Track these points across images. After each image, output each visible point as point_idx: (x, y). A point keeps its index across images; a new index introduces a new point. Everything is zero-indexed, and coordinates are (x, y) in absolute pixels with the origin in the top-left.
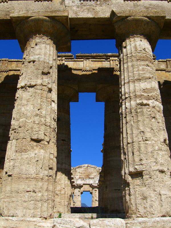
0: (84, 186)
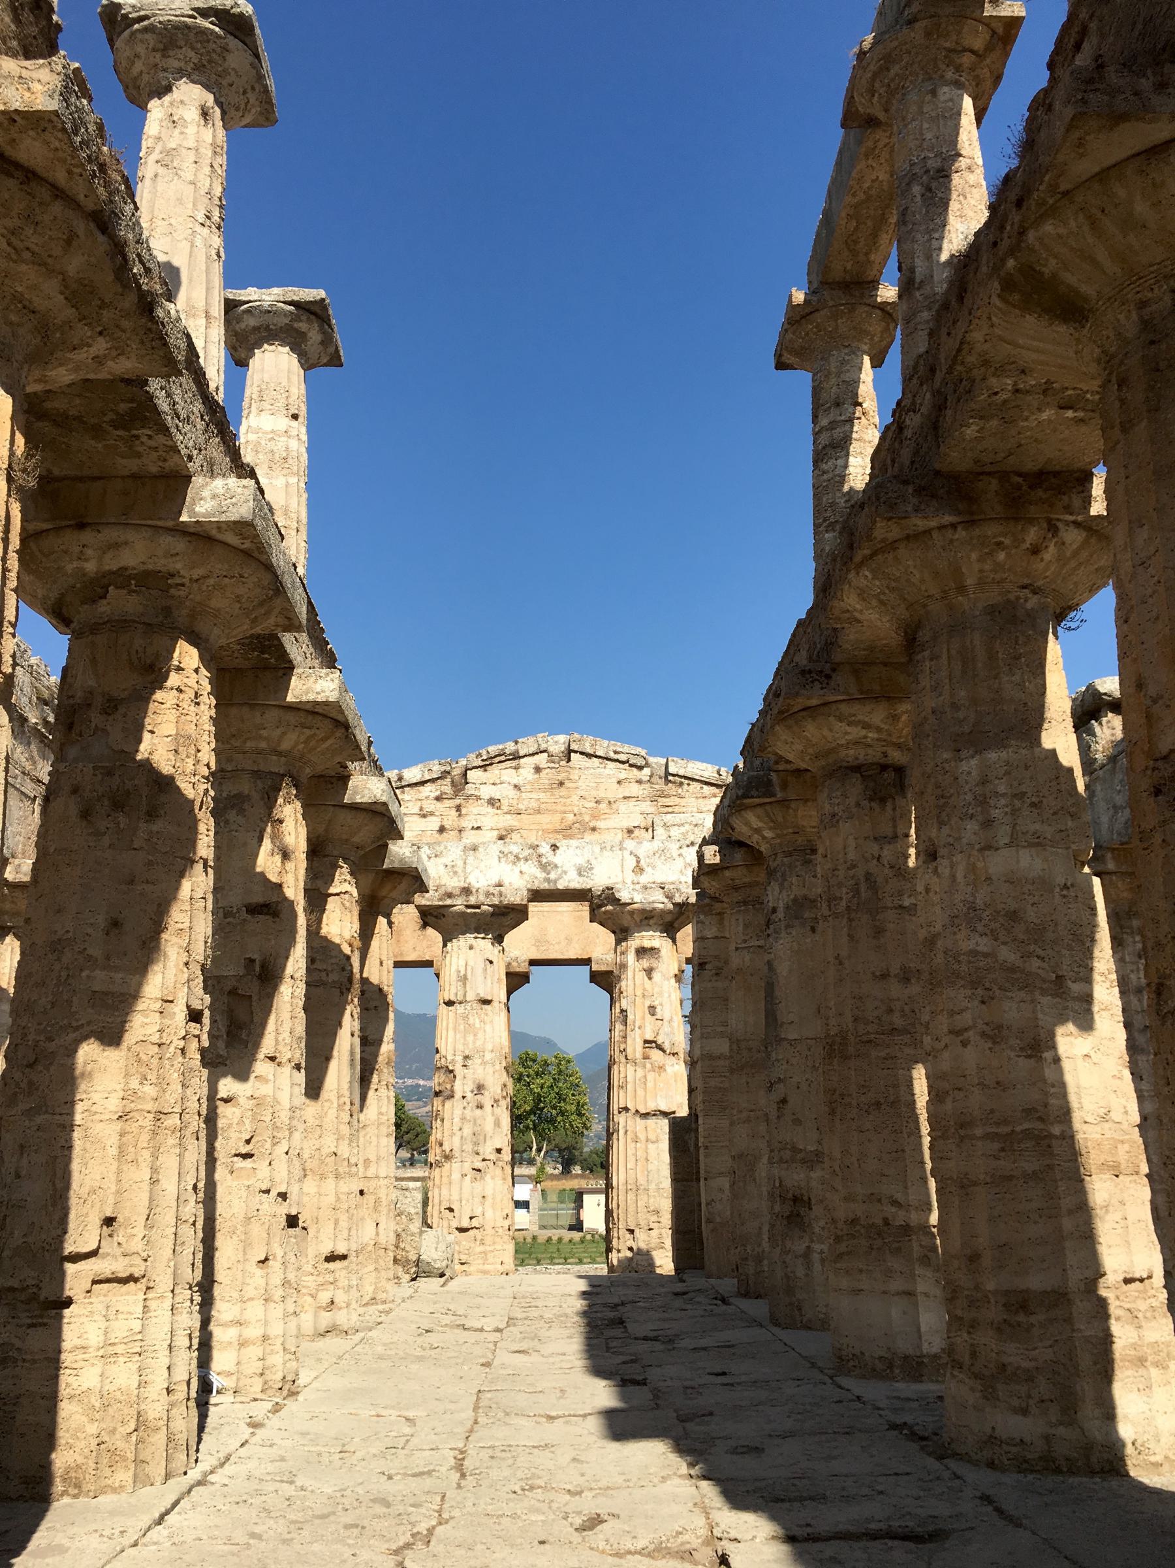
0: (533, 908)
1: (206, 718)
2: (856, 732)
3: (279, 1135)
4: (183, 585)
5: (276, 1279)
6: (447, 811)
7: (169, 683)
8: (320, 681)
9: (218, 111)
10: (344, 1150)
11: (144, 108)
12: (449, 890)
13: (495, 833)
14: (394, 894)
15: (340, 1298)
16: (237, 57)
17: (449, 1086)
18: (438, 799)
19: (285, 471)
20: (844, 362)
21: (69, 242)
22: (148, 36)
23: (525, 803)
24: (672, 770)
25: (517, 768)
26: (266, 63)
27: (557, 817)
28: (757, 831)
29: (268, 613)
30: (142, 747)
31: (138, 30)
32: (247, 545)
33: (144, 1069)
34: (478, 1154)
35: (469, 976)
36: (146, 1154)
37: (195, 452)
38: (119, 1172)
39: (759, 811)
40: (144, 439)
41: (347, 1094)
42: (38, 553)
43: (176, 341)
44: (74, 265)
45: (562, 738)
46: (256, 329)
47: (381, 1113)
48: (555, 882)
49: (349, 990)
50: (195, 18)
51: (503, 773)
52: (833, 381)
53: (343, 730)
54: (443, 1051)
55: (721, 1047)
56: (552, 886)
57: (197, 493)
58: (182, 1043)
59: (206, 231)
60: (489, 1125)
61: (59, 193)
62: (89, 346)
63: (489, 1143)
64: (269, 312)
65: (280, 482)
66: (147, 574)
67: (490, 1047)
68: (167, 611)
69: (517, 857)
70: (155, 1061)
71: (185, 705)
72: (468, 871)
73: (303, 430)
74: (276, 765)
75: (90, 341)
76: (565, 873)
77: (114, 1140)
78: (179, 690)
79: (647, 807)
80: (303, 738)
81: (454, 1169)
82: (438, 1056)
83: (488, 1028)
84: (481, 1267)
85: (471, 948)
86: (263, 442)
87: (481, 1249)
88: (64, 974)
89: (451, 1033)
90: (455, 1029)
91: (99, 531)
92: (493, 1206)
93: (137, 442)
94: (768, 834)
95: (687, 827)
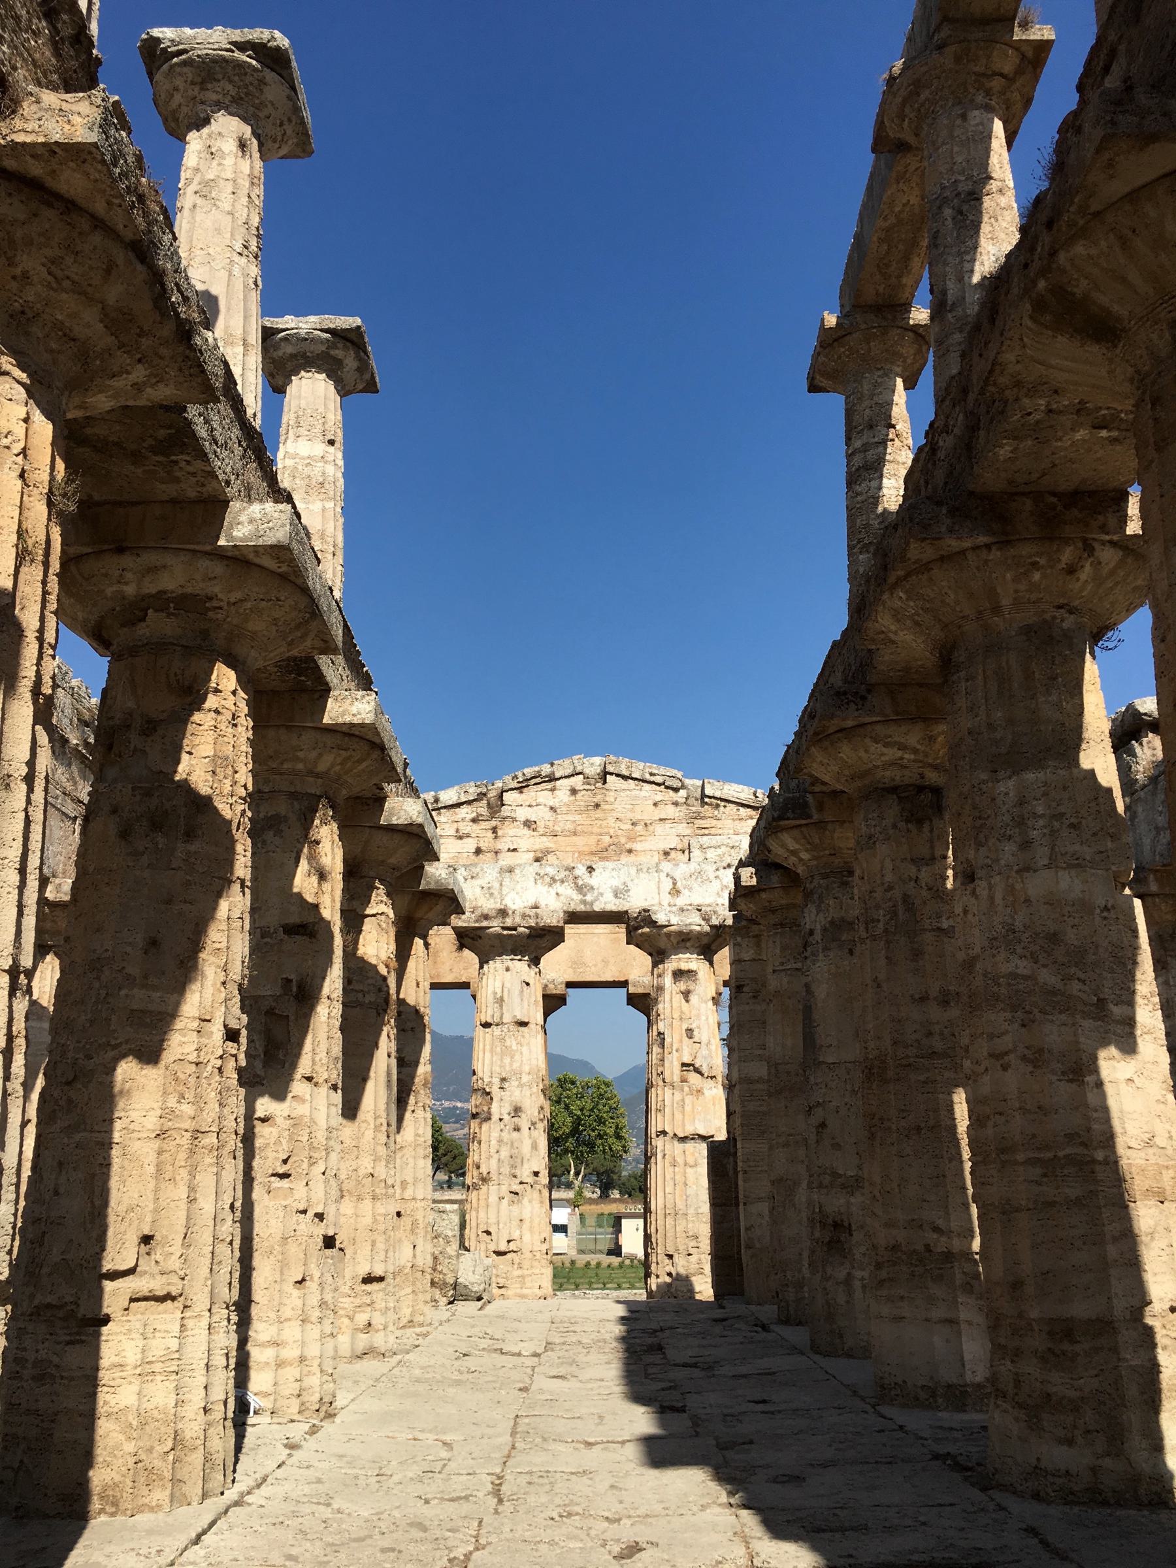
0: (569, 930)
1: (243, 740)
2: (892, 753)
3: (316, 1155)
4: (221, 608)
5: (314, 1300)
6: (483, 834)
7: (207, 705)
8: (356, 703)
9: (255, 142)
10: (381, 1171)
11: (182, 139)
12: (486, 912)
13: (531, 855)
14: (430, 915)
15: (378, 1320)
16: (274, 90)
17: (485, 1109)
18: (474, 821)
19: (322, 496)
20: (876, 385)
21: (108, 271)
22: (186, 70)
23: (561, 824)
24: (709, 791)
25: (553, 790)
26: (302, 96)
27: (592, 840)
28: (794, 853)
29: (304, 637)
30: (180, 768)
31: (176, 64)
32: (284, 568)
33: (181, 1088)
34: (515, 1177)
35: (506, 998)
36: (184, 1173)
37: (233, 478)
38: (156, 1191)
39: (796, 832)
40: (183, 464)
41: (384, 1115)
42: (78, 576)
43: (214, 369)
44: (114, 293)
45: (598, 760)
46: (293, 356)
47: (418, 1135)
48: (592, 904)
49: (385, 1011)
50: (233, 51)
51: (539, 795)
52: (867, 403)
53: (379, 752)
54: (480, 1074)
55: (760, 1070)
56: (588, 909)
57: (235, 518)
58: (219, 1062)
59: (243, 260)
60: (526, 1148)
61: (98, 224)
62: (128, 373)
63: (526, 1166)
64: (306, 339)
65: (317, 506)
66: (184, 597)
67: (526, 1069)
68: (205, 634)
69: (553, 880)
70: (192, 1080)
71: (222, 726)
72: (504, 893)
73: (340, 455)
74: (313, 787)
75: (129, 368)
76: (602, 894)
77: (152, 1158)
78: (217, 712)
79: (683, 828)
80: (339, 760)
81: (491, 1192)
82: (475, 1078)
83: (525, 1049)
84: (518, 1291)
85: (508, 969)
86: (300, 467)
87: (519, 1272)
88: (103, 992)
89: (488, 1055)
90: (492, 1051)
91: (138, 555)
92: (531, 1229)
93: (176, 468)
94: (805, 856)
95: (723, 849)
